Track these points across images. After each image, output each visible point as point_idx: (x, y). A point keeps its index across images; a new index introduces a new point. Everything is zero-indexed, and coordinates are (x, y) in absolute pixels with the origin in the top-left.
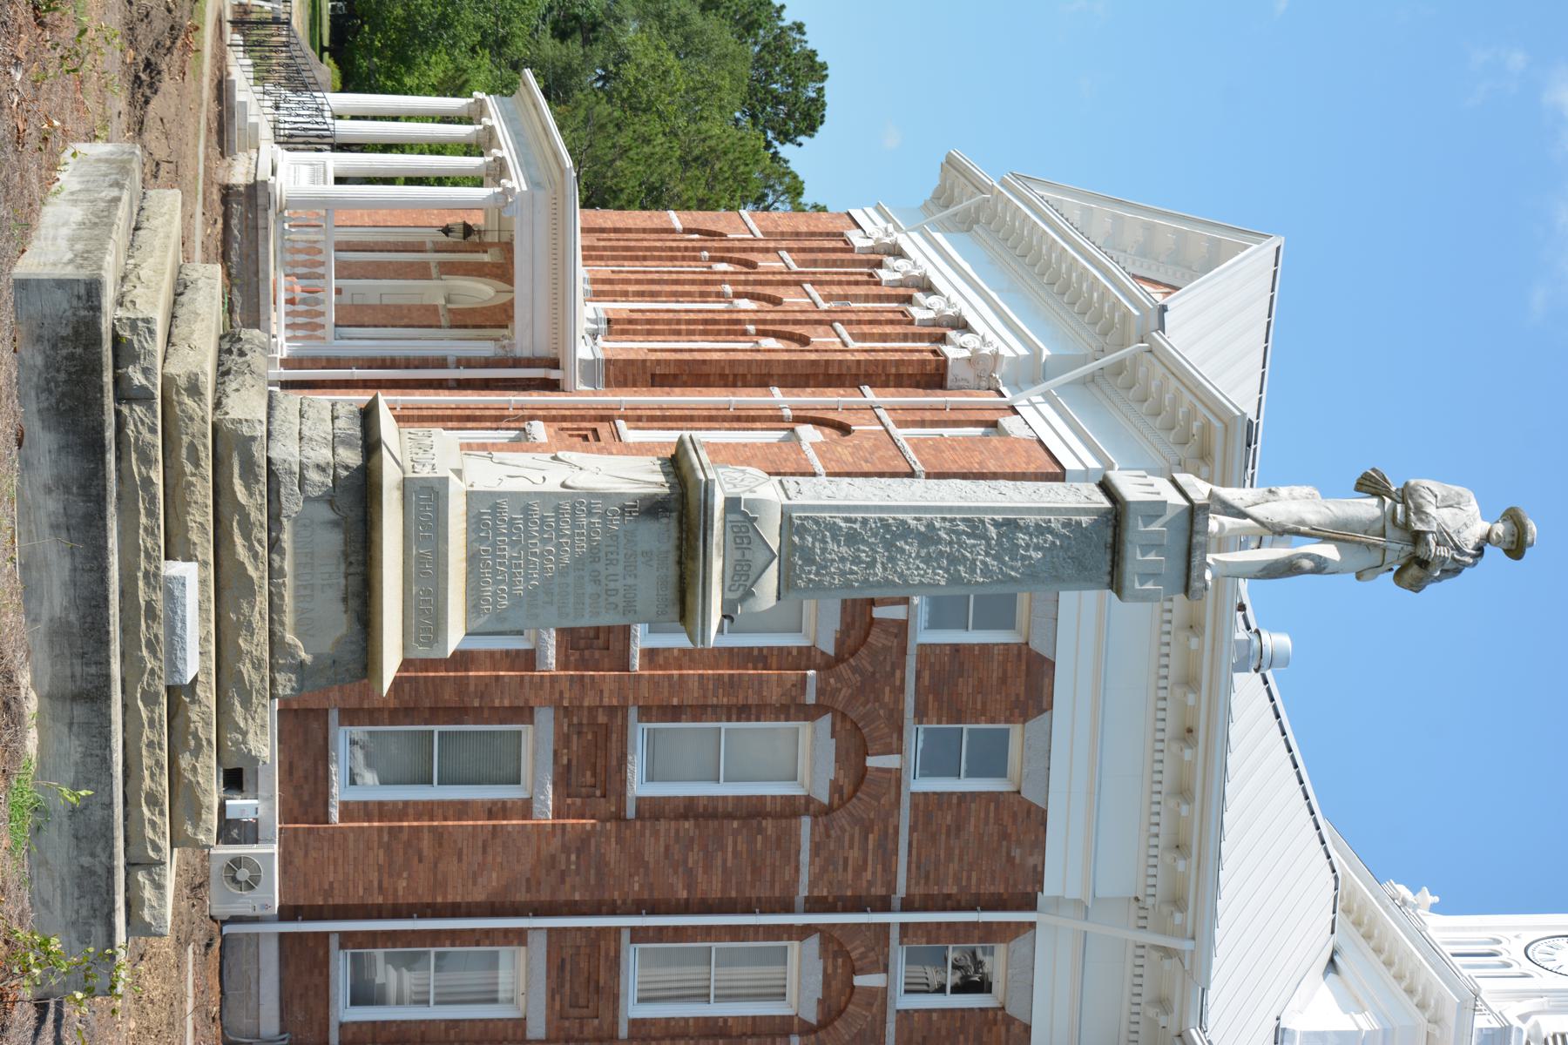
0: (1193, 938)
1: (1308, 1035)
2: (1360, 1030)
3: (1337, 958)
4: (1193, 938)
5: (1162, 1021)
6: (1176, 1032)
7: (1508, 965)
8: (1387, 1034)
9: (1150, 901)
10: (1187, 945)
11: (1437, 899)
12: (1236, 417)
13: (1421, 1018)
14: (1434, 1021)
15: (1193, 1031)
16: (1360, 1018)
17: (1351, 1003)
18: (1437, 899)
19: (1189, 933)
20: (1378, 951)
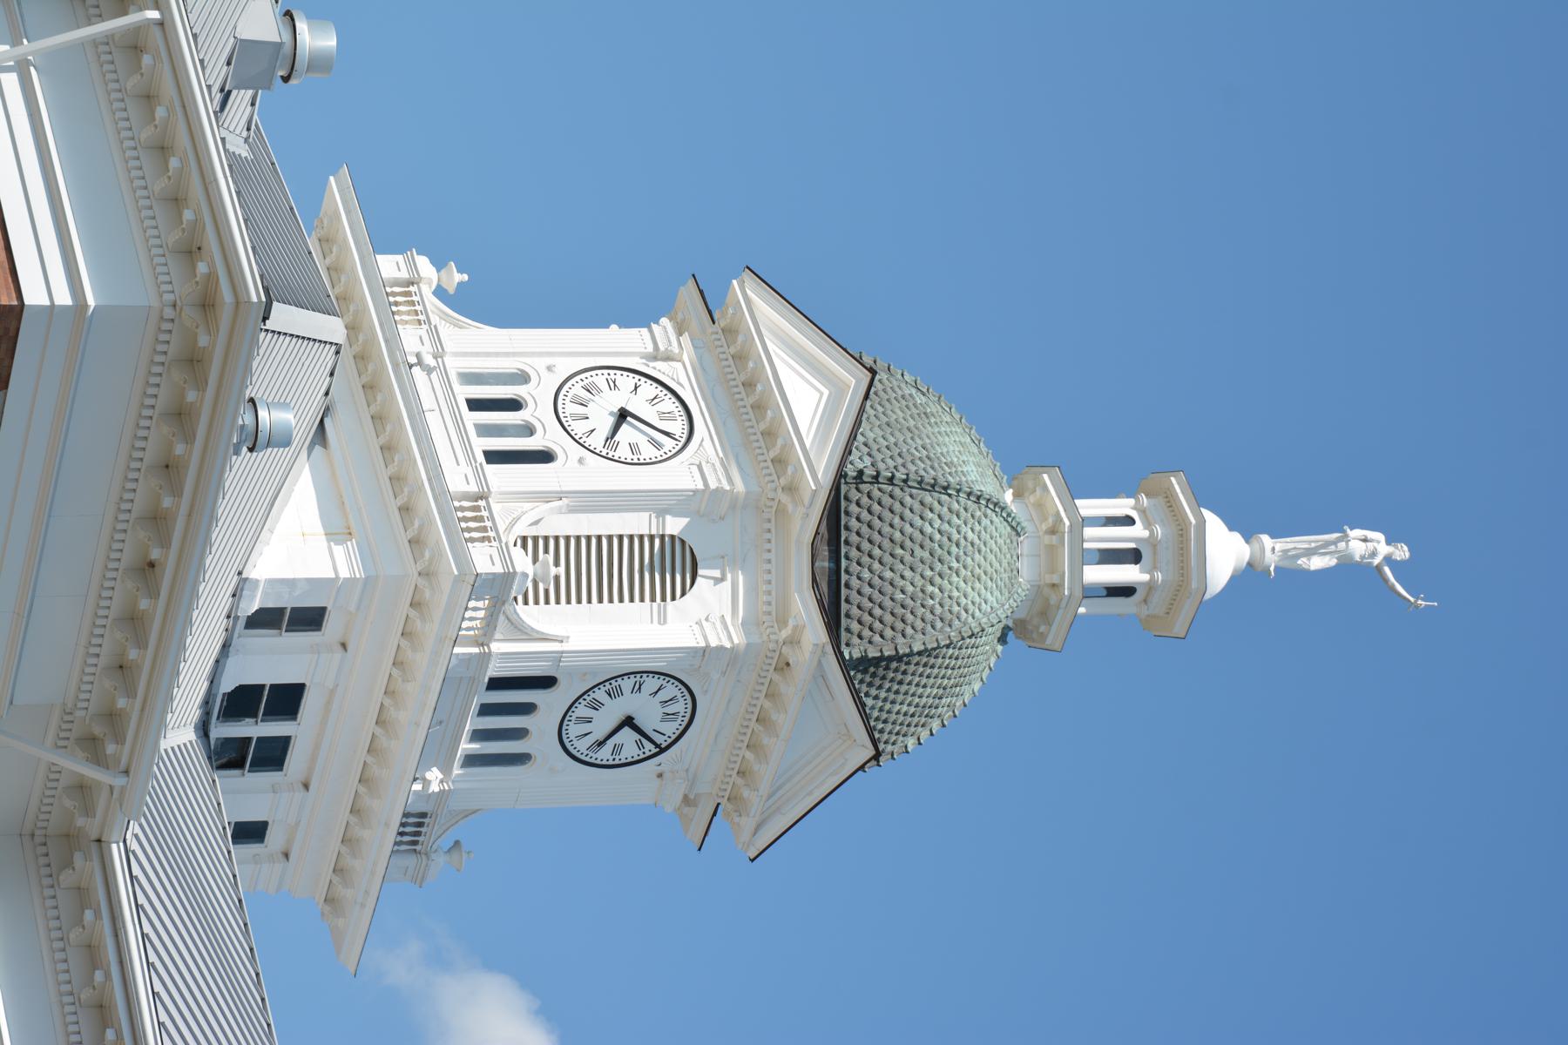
0: (127, 772)
1: (272, 582)
2: (337, 578)
3: (327, 421)
4: (127, 772)
5: (80, 822)
6: (94, 836)
7: (529, 430)
8: (369, 582)
9: (80, 714)
10: (119, 781)
11: (466, 277)
12: (249, 302)
13: (413, 570)
14: (425, 574)
15: (114, 846)
16: (339, 551)
17: (337, 532)
18: (466, 277)
19: (123, 766)
20: (378, 419)
